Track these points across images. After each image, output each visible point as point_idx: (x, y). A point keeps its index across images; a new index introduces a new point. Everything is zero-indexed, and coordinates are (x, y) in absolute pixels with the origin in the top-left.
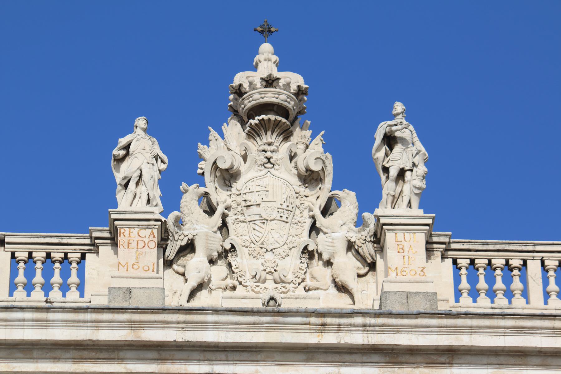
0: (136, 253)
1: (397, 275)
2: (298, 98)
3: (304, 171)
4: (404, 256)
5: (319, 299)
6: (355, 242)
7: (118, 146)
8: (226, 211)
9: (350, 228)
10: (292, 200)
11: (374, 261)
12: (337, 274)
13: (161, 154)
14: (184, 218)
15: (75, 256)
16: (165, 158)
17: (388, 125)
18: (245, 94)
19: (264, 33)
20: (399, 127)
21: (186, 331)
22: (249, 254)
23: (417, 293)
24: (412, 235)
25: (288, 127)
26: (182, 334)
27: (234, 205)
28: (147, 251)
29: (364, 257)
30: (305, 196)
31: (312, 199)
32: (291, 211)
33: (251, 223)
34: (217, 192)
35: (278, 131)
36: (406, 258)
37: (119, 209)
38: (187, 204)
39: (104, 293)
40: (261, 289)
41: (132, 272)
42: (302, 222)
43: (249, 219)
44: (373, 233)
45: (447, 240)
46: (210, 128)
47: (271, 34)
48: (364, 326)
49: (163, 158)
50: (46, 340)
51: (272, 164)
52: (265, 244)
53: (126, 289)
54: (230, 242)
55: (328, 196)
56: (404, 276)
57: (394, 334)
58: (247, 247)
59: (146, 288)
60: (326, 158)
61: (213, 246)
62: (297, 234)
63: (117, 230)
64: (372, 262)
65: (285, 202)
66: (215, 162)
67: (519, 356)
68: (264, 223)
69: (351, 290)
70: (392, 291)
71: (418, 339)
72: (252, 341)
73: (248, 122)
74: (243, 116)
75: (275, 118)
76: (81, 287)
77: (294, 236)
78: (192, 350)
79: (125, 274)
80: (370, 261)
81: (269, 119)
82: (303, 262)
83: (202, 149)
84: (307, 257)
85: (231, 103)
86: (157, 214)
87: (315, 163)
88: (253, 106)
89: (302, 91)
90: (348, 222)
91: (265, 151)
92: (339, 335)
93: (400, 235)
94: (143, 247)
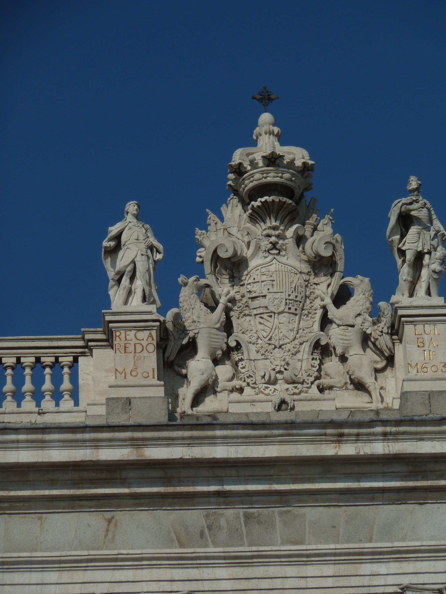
0: (134, 357)
1: (418, 372)
3: (312, 256)
4: (424, 351)
5: (334, 400)
6: (371, 334)
7: (109, 236)
10: (301, 289)
11: (392, 354)
12: (353, 370)
13: (156, 243)
14: (184, 314)
15: (67, 360)
16: (160, 247)
17: (403, 203)
19: (264, 101)
20: (415, 206)
21: (193, 448)
22: (256, 350)
23: (440, 392)
24: (432, 326)
25: (294, 209)
26: (188, 450)
27: (238, 297)
28: (146, 355)
30: (315, 284)
31: (323, 287)
32: (300, 302)
33: (257, 316)
34: (218, 284)
35: (283, 214)
37: (114, 308)
38: (187, 298)
39: (100, 402)
40: (271, 390)
41: (131, 380)
42: (313, 313)
43: (255, 312)
44: (390, 325)
46: (207, 210)
47: (271, 102)
48: (385, 434)
49: (158, 248)
50: (43, 462)
51: (277, 249)
52: (273, 339)
54: (235, 339)
55: (340, 283)
56: (425, 373)
57: (416, 441)
58: (254, 344)
59: (146, 397)
60: (337, 241)
61: (217, 344)
62: (306, 327)
63: (112, 332)
65: (294, 292)
66: (215, 251)
68: (271, 316)
69: (368, 387)
70: (413, 391)
71: (442, 446)
72: (264, 455)
73: (249, 204)
74: (244, 197)
75: (279, 199)
77: (305, 329)
79: (123, 383)
80: (388, 354)
81: (273, 200)
82: (315, 358)
83: (199, 233)
84: (319, 352)
85: (230, 182)
86: (155, 314)
87: (325, 248)
88: (255, 187)
89: (308, 168)
90: (363, 312)
91: (269, 236)
92: (358, 445)
93: (420, 328)
94: (141, 351)
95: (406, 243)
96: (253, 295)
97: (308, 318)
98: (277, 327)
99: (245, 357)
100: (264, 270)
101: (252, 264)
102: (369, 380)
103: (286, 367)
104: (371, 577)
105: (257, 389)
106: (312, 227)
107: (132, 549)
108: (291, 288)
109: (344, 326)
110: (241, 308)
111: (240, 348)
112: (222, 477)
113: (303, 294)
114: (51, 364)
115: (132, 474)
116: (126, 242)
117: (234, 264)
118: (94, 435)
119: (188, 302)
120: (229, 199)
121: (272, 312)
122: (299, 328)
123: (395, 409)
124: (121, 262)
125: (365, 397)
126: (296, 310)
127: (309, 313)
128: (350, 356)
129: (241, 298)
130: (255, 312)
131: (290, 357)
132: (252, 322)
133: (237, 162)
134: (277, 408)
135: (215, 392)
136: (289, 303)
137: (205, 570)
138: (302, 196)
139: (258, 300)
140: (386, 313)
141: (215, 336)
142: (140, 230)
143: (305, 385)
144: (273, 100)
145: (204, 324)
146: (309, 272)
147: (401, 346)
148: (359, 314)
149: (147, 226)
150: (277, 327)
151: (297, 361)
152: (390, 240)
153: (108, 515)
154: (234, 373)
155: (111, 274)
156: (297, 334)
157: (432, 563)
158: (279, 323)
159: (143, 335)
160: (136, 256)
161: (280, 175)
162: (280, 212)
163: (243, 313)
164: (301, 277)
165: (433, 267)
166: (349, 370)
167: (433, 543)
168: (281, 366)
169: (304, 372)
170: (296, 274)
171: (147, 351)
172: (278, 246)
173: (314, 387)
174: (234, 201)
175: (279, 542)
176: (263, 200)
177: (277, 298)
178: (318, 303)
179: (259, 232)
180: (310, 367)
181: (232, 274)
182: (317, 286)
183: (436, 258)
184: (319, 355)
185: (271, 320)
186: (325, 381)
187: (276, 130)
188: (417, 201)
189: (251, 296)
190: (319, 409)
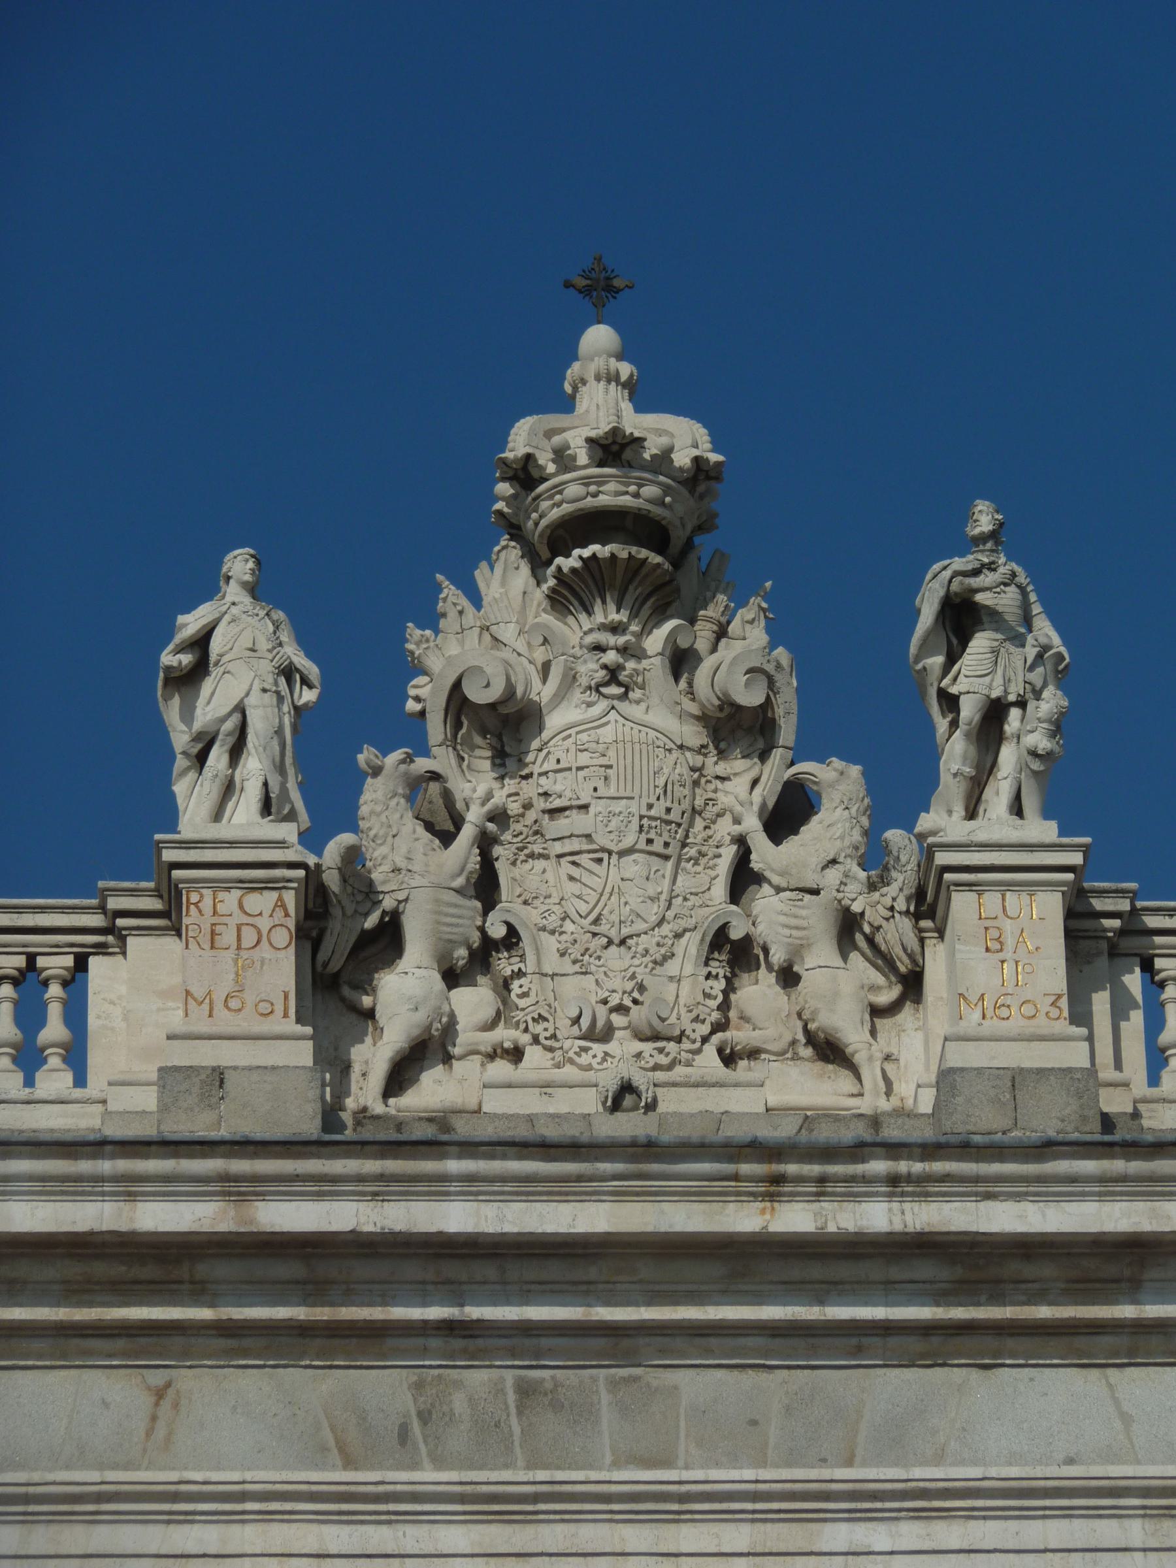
0: (236, 961)
1: (984, 1017)
2: (695, 491)
3: (713, 706)
4: (1003, 962)
5: (762, 1086)
6: (862, 914)
7: (179, 638)
8: (491, 826)
9: (851, 874)
10: (680, 792)
11: (918, 969)
13: (301, 661)
14: (370, 850)
15: (56, 964)
16: (312, 670)
18: (542, 483)
19: (595, 294)
21: (386, 1204)
22: (558, 950)
23: (1041, 1072)
24: (1025, 897)
25: (667, 578)
27: (514, 808)
28: (267, 956)
29: (889, 957)
30: (717, 777)
31: (739, 786)
32: (679, 825)
33: (563, 860)
34: (463, 771)
35: (639, 590)
38: (378, 808)
39: (143, 1077)
40: (594, 1056)
41: (225, 1021)
42: (710, 855)
43: (558, 848)
44: (913, 891)
45: (1124, 905)
46: (439, 577)
47: (615, 298)
48: (894, 1180)
49: (306, 672)
51: (620, 684)
52: (604, 921)
53: (209, 1072)
54: (504, 919)
55: (785, 779)
57: (976, 1201)
58: (553, 932)
59: (266, 1068)
60: (779, 666)
62: (693, 890)
64: (912, 972)
65: (662, 797)
66: (457, 685)
69: (853, 1055)
70: (971, 1068)
71: (1044, 1216)
72: (574, 1228)
73: (549, 563)
74: (537, 545)
75: (630, 553)
77: (688, 896)
79: (204, 1027)
80: (906, 967)
81: (613, 555)
82: (714, 973)
83: (415, 637)
84: (724, 957)
85: (500, 505)
86: (294, 849)
87: (748, 684)
88: (566, 518)
89: (707, 471)
90: (843, 854)
91: (599, 648)
92: (822, 1208)
93: (992, 900)
94: (256, 946)
95: (961, 676)
96: (555, 802)
97: (699, 869)
98: (616, 890)
99: (530, 966)
100: (584, 737)
101: (554, 721)
102: (853, 1036)
103: (636, 995)
104: (850, 1557)
105: (559, 1053)
106: (715, 628)
107: (218, 1468)
108: (656, 786)
109: (792, 890)
110: (521, 837)
111: (517, 944)
112: (461, 1283)
113: (686, 805)
114: (15, 973)
115: (222, 1270)
116: (221, 656)
117: (506, 720)
118: (123, 1165)
119: (383, 818)
120: (496, 549)
121: (603, 850)
122: (673, 894)
123: (922, 1115)
124: (208, 709)
125: (844, 1081)
126: (666, 845)
127: (701, 854)
128: (807, 970)
129: (521, 810)
130: (558, 848)
131: (648, 970)
132: (550, 876)
133: (521, 451)
134: (609, 1103)
135: (447, 1059)
136: (650, 827)
137: (410, 1530)
138: (689, 545)
139: (567, 817)
140: (903, 859)
141: (452, 911)
142: (258, 625)
143: (686, 1045)
144: (618, 291)
145: (423, 876)
146: (703, 746)
147: (941, 948)
148: (834, 862)
149: (279, 615)
150: (616, 890)
151: (665, 979)
152: (919, 667)
153: (157, 1378)
154: (499, 1009)
155: (181, 739)
156: (669, 908)
157: (1013, 1525)
158: (622, 879)
160: (247, 694)
161: (632, 488)
162: (631, 588)
163: (526, 851)
164: (682, 759)
165: (1030, 740)
166: (803, 1009)
167: (1014, 1472)
168: (624, 992)
169: (683, 1011)
170: (670, 750)
171: (271, 944)
172: (623, 677)
173: (710, 1050)
174: (510, 554)
175: (608, 1459)
176: (586, 553)
177: (617, 812)
178: (725, 829)
179: (575, 639)
180: (700, 998)
181: (499, 747)
182: (722, 783)
183: (1039, 719)
184: (723, 967)
186: (738, 1036)
187: (626, 370)
188: (993, 566)
189: (549, 806)
190: (722, 1110)
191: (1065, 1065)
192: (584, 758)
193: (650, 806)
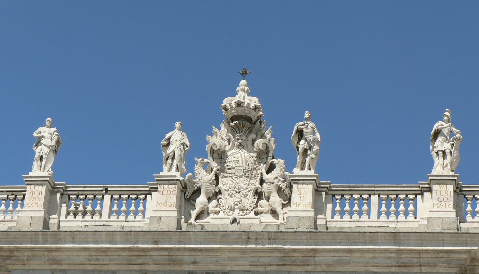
1: (296, 207)
10: (251, 165)
16: (188, 144)
32: (251, 171)
36: (302, 198)
38: (197, 169)
41: (163, 208)
42: (257, 176)
43: (229, 175)
67: (349, 252)
68: (236, 178)
76: (144, 212)
78: (185, 251)
85: (224, 113)
93: (300, 186)
103: (240, 202)
119: (198, 170)
121: (237, 176)
126: (248, 175)
127: (255, 176)
149: (184, 133)
159: (172, 186)
160: (175, 149)
162: (244, 129)
165: (311, 156)
168: (238, 202)
170: (250, 157)
173: (253, 212)
178: (259, 172)
180: (252, 202)
185: (236, 179)
186: (259, 209)
187: (246, 88)
191: (309, 216)
192: (234, 159)
193: (246, 168)
